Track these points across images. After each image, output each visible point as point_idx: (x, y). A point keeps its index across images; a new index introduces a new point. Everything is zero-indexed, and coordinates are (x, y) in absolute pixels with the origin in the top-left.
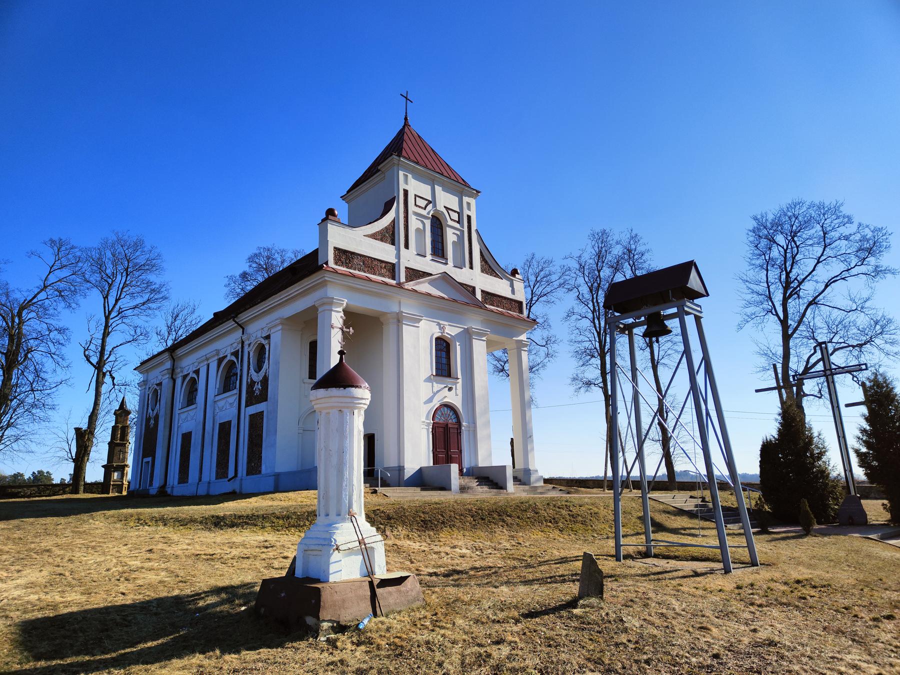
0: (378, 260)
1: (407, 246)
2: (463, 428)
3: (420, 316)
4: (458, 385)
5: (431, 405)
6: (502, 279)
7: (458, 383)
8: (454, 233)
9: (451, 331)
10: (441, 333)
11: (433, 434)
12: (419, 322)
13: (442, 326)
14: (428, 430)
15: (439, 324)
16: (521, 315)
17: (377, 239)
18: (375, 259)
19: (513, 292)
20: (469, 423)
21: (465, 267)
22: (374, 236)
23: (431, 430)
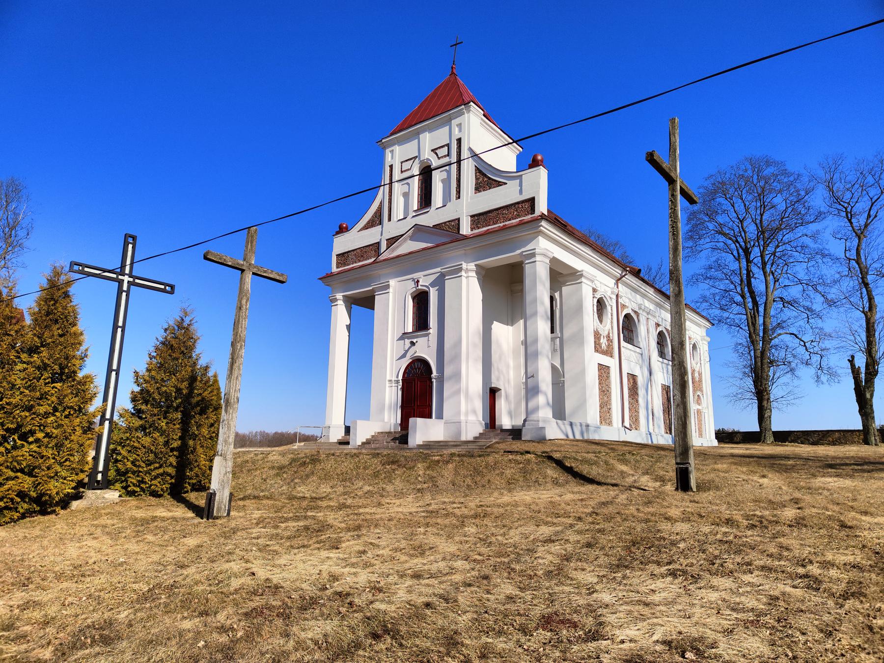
0: (366, 246)
1: (390, 220)
6: (506, 184)
7: (430, 333)
8: (441, 172)
9: (425, 279)
13: (416, 280)
15: (414, 280)
16: (533, 215)
19: (521, 192)
21: (450, 201)
22: (366, 227)
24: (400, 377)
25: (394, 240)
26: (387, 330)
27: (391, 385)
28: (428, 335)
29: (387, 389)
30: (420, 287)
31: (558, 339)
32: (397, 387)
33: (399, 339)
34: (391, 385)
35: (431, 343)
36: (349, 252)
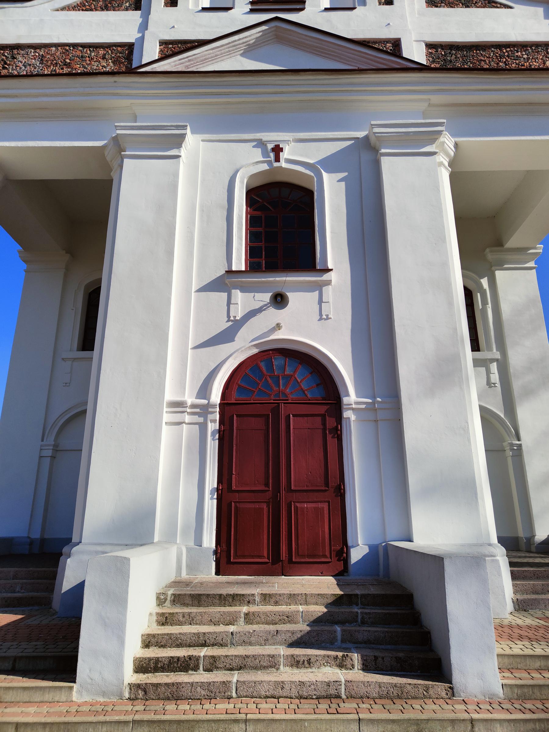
2: (347, 414)
3: (178, 127)
4: (329, 292)
5: (225, 349)
6: (511, 7)
7: (329, 283)
10: (269, 163)
11: (221, 440)
12: (179, 146)
13: (270, 146)
14: (203, 427)
15: (261, 144)
17: (91, 10)
18: (75, 46)
20: (374, 397)
23: (213, 426)
24: (216, 396)
25: (182, 47)
26: (170, 253)
27: (177, 418)
28: (319, 287)
29: (165, 429)
30: (283, 164)
31: (495, 364)
32: (203, 427)
33: (203, 289)
34: (177, 418)
35: (328, 309)
36: (18, 47)
